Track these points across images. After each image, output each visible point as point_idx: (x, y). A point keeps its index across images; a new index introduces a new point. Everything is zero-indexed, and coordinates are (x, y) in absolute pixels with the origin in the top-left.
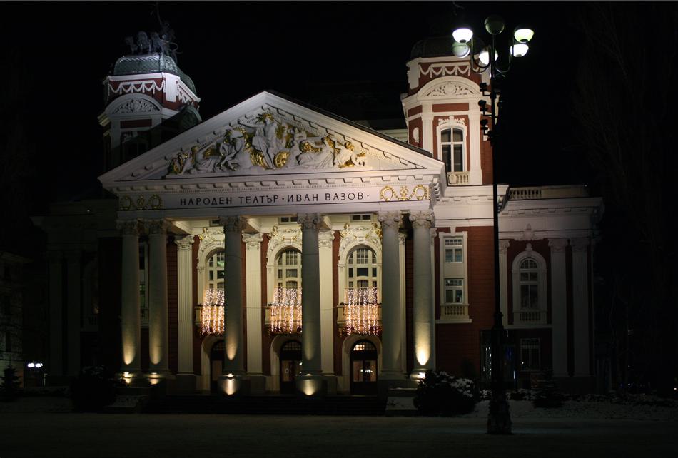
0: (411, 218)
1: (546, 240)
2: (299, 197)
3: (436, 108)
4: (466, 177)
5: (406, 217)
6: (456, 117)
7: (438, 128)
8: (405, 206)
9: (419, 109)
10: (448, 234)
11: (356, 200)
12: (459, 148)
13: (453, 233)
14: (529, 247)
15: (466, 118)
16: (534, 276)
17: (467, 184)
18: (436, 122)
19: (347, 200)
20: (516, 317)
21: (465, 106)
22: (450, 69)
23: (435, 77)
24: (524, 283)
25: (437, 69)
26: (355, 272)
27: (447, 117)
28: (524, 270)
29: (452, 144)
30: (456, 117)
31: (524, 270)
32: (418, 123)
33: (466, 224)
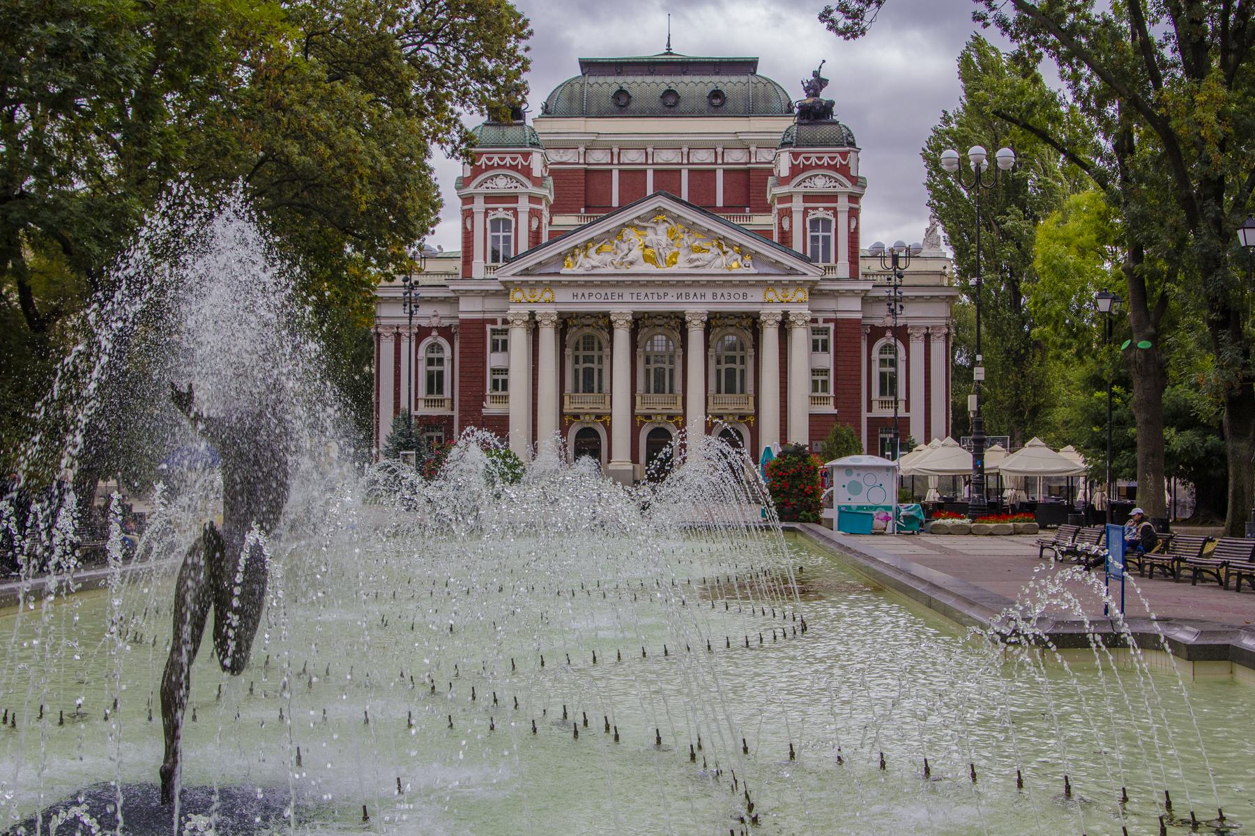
0: (791, 318)
1: (905, 327)
2: (687, 295)
3: (807, 198)
4: (834, 268)
5: (786, 314)
6: (826, 209)
7: (808, 220)
8: (786, 307)
9: (788, 198)
10: (815, 325)
11: (741, 300)
12: (826, 240)
13: (821, 325)
14: (889, 334)
15: (835, 209)
16: (893, 363)
17: (834, 276)
18: (806, 212)
19: (733, 300)
20: (875, 405)
21: (833, 198)
22: (820, 159)
23: (807, 168)
24: (884, 369)
25: (807, 159)
26: (723, 361)
27: (817, 209)
28: (883, 356)
29: (820, 234)
30: (826, 209)
31: (883, 356)
32: (788, 213)
33: (832, 316)
